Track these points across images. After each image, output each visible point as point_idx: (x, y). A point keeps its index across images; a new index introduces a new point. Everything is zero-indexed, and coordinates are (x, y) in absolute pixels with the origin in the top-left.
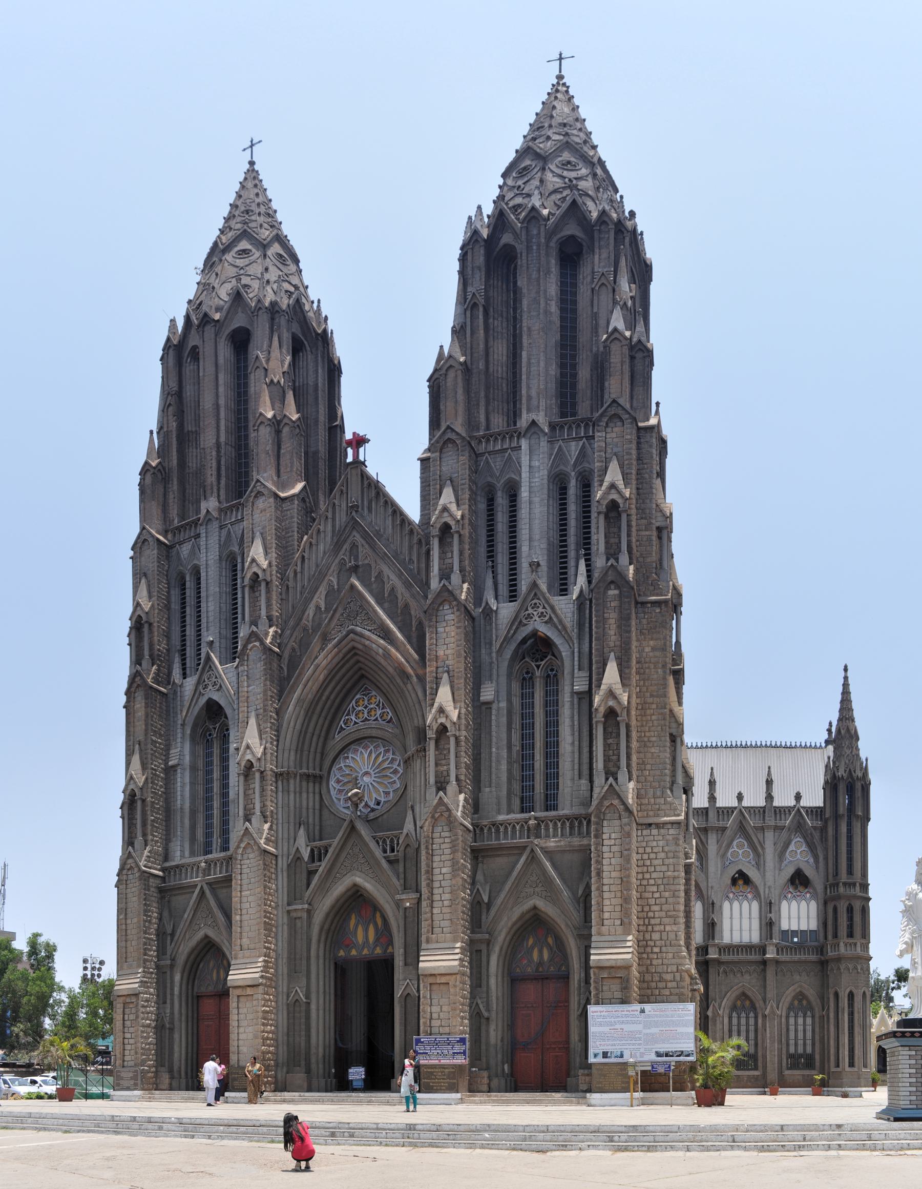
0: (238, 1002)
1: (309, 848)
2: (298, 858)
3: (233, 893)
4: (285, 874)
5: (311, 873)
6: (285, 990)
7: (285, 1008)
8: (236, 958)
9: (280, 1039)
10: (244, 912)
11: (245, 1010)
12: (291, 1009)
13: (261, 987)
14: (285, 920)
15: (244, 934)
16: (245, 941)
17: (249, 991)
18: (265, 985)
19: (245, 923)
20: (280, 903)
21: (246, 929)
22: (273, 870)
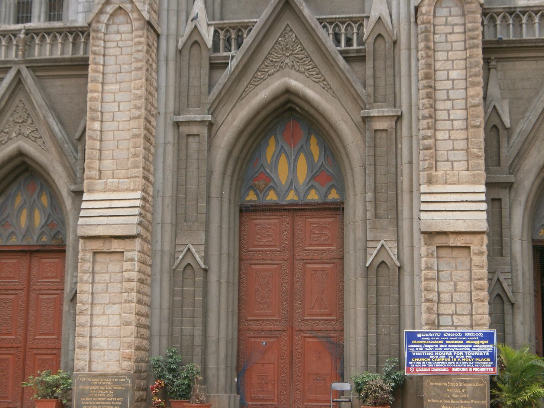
0: (94, 263)
1: (212, 29)
2: (196, 42)
3: (90, 86)
4: (172, 65)
5: (216, 66)
6: (167, 248)
7: (166, 276)
8: (90, 191)
9: (156, 328)
10: (107, 116)
11: (107, 277)
12: (179, 279)
13: (138, 241)
14: (170, 137)
15: (106, 153)
16: (108, 164)
17: (116, 245)
18: (145, 240)
19: (108, 136)
20: (162, 111)
21: (109, 144)
22: (154, 55)
